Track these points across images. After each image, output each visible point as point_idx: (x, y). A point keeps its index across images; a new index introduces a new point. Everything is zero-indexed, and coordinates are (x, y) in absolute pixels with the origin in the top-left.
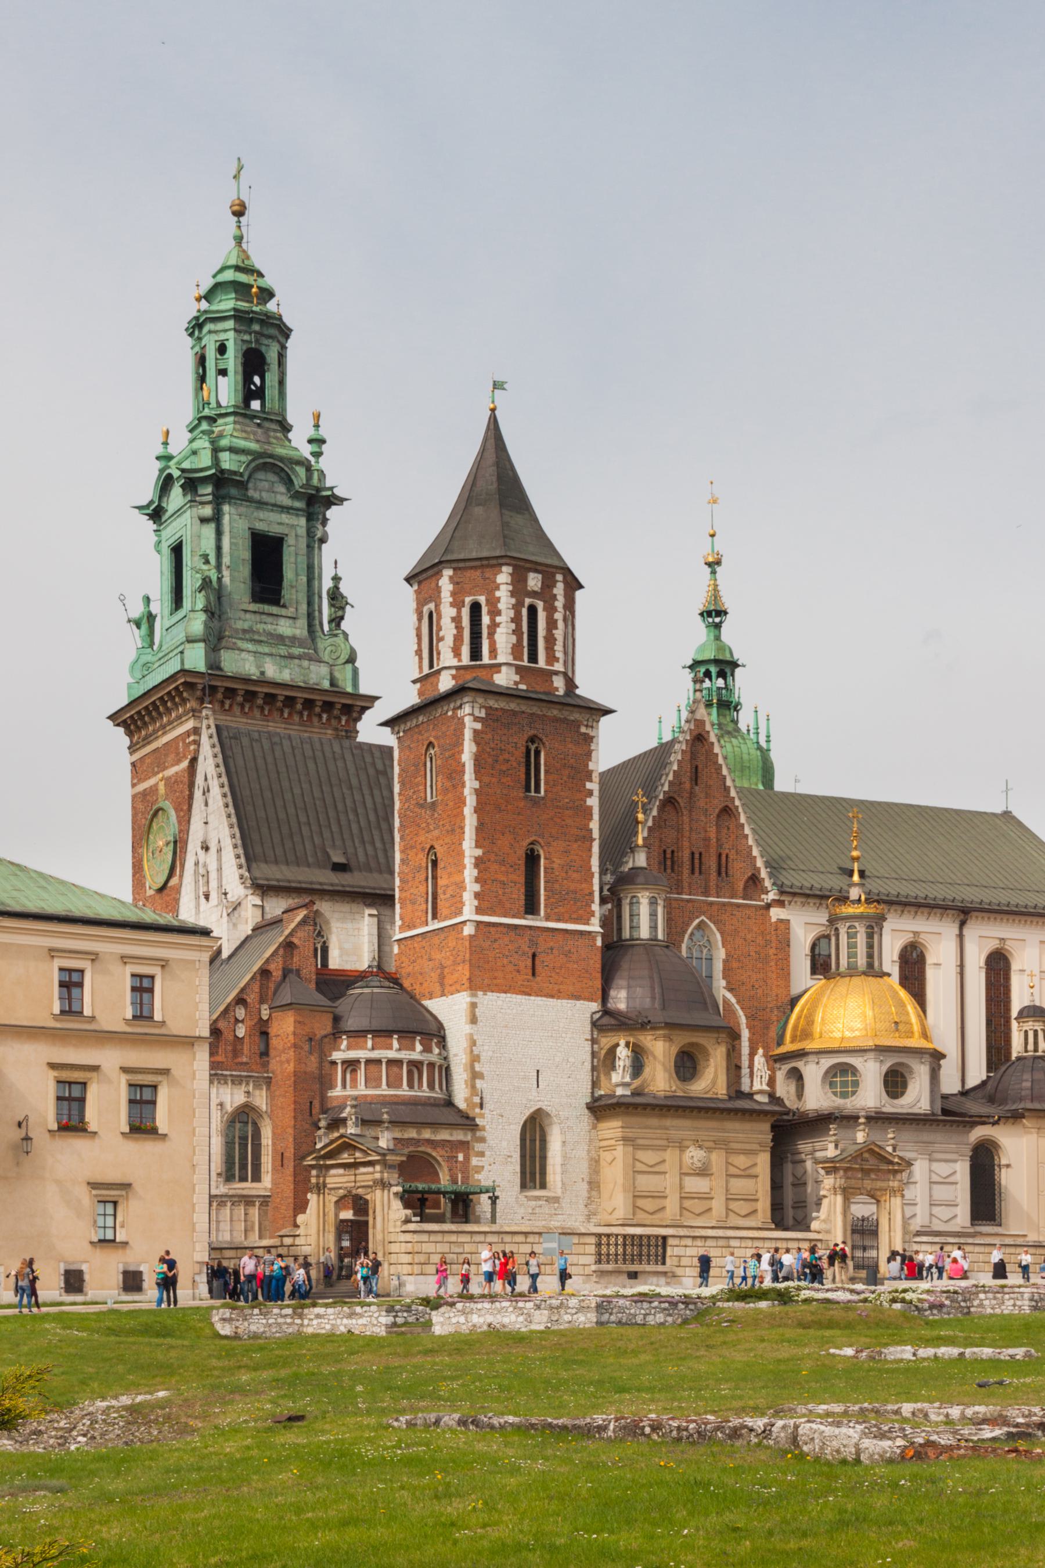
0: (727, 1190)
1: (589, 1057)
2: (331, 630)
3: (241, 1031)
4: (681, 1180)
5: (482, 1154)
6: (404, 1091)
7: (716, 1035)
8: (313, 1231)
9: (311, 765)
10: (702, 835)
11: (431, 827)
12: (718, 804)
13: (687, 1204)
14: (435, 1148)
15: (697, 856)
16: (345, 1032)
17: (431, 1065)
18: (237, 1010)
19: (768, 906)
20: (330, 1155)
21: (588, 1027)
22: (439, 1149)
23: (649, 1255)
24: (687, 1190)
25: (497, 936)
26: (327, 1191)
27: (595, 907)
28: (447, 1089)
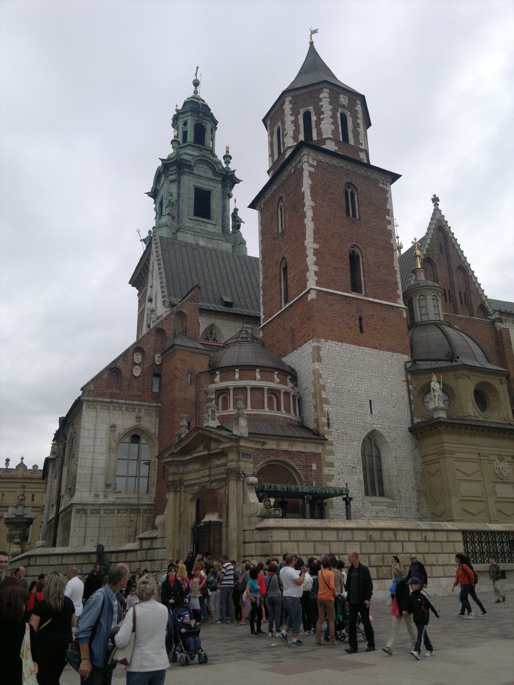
2: (234, 232)
3: (137, 372)
5: (332, 465)
6: (266, 411)
7: (500, 378)
8: (169, 532)
10: (449, 281)
11: (282, 247)
15: (447, 292)
16: (218, 369)
17: (286, 394)
20: (185, 451)
21: (403, 373)
22: (296, 459)
26: (183, 488)
27: (400, 292)
28: (300, 414)
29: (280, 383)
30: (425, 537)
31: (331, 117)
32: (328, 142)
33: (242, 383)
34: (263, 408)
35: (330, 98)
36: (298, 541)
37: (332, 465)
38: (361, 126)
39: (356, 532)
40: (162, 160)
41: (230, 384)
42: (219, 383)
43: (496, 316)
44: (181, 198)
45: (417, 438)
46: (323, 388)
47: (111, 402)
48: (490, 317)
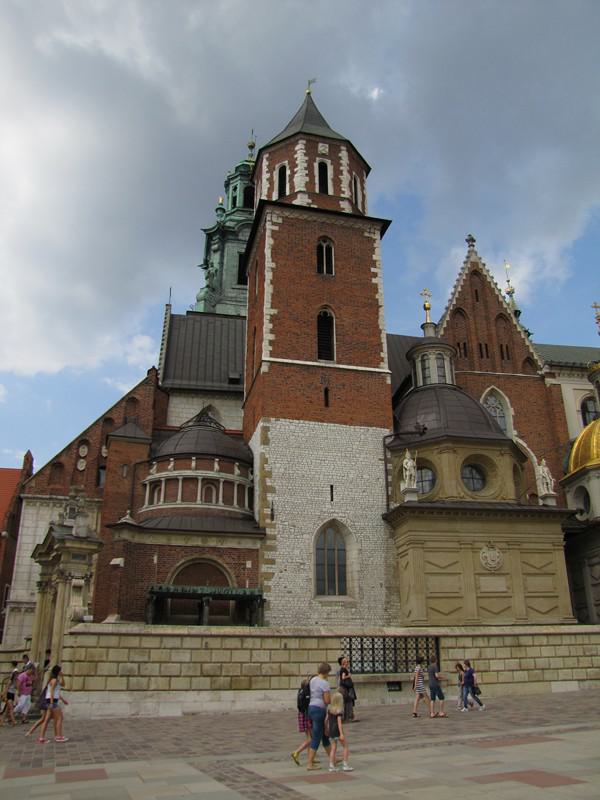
0: (525, 588)
1: (383, 476)
3: (82, 465)
4: (475, 579)
5: (272, 562)
6: (199, 504)
9: (232, 333)
10: (486, 333)
12: (494, 312)
13: (485, 603)
14: (221, 556)
15: (483, 346)
16: (155, 459)
18: (81, 449)
19: (543, 378)
21: (381, 449)
23: (406, 662)
24: (483, 590)
25: (290, 374)
27: (384, 354)
29: (220, 471)
30: (285, 645)
31: (306, 169)
32: (299, 196)
33: (175, 473)
34: (195, 500)
35: (305, 149)
36: (108, 648)
37: (272, 562)
38: (345, 173)
39: (188, 639)
40: (205, 230)
41: (164, 474)
42: (155, 474)
43: (546, 370)
44: (225, 267)
45: (392, 526)
46: (269, 474)
47: (50, 499)
48: (540, 372)
